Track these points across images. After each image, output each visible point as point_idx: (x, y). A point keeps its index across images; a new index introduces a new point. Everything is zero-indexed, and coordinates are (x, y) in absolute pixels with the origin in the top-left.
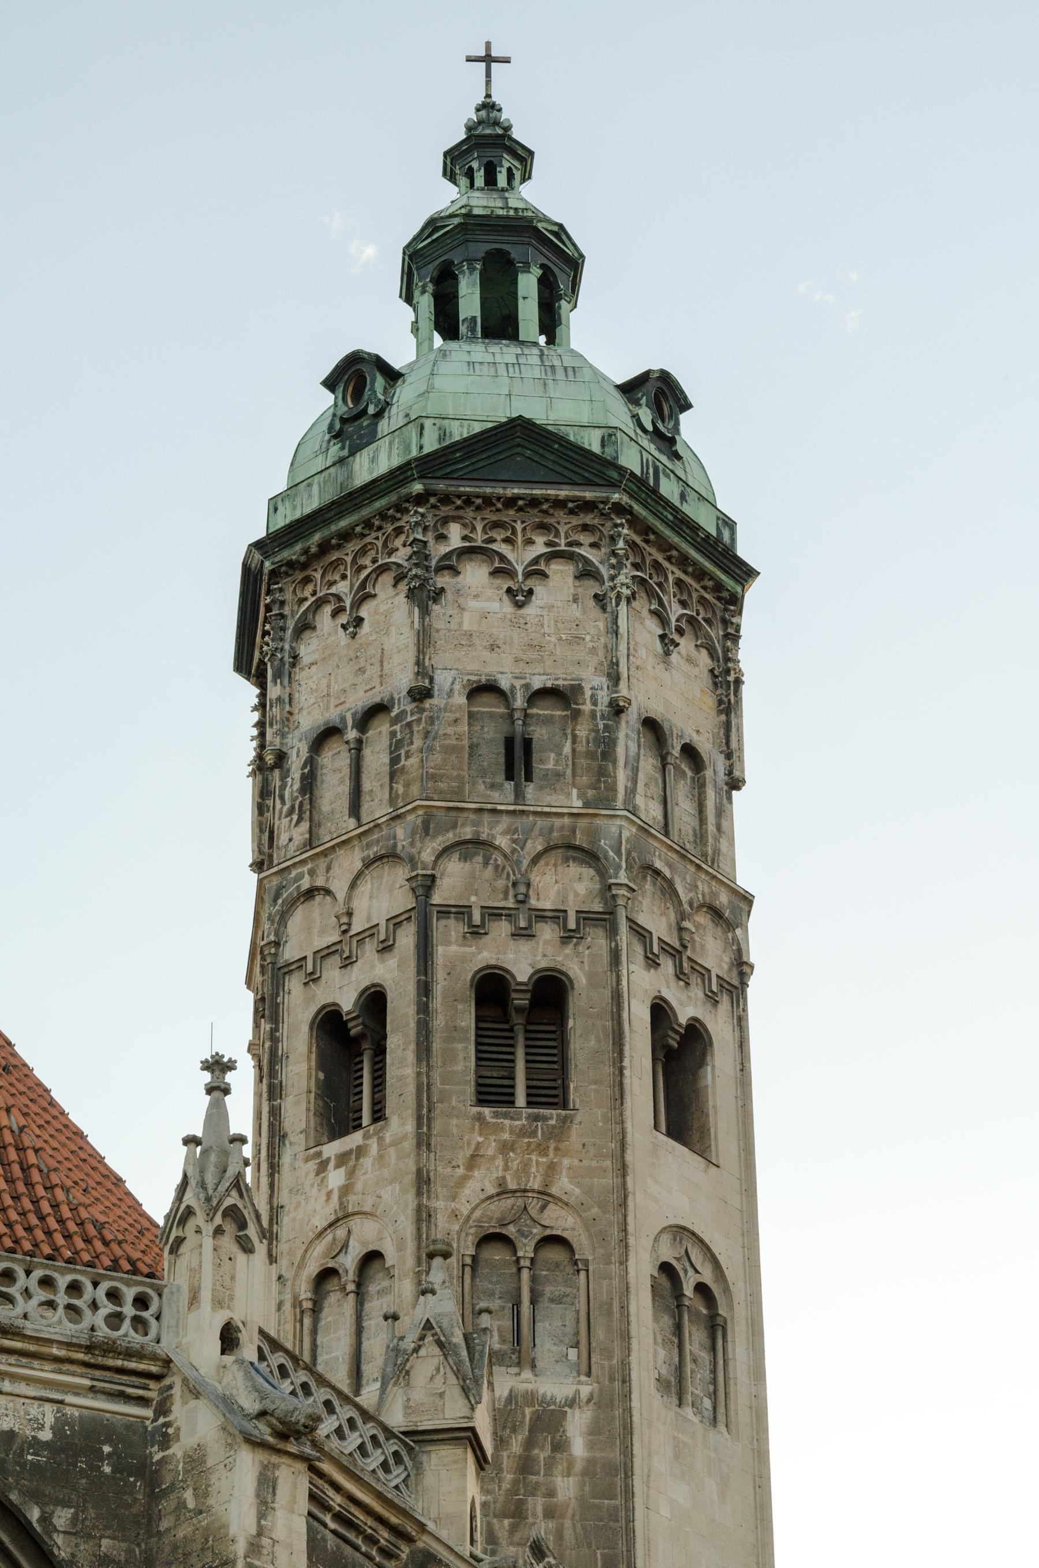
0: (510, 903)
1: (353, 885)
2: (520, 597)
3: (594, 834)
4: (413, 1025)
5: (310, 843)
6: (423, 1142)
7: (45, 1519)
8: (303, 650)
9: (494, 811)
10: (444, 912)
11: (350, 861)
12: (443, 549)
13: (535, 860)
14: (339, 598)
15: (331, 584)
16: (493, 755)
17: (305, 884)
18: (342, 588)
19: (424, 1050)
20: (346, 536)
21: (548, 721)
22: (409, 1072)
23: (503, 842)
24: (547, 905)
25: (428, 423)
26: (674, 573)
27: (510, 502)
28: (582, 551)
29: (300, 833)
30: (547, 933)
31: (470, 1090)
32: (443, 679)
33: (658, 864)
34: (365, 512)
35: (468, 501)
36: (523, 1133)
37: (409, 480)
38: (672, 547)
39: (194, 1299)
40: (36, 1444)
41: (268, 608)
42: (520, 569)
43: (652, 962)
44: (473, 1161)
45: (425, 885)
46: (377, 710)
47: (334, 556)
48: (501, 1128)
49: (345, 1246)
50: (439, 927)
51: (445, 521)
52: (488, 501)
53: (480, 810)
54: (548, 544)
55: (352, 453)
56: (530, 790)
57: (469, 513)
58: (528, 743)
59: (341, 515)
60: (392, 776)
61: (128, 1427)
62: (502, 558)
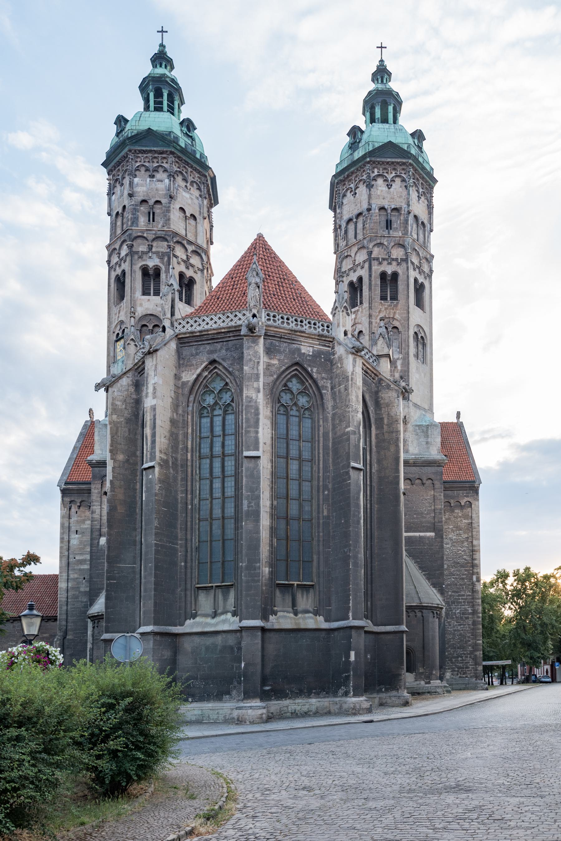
0: (387, 257)
1: (356, 254)
2: (389, 186)
3: (404, 241)
4: (368, 284)
5: (346, 245)
6: (370, 308)
8: (344, 201)
10: (374, 259)
11: (355, 249)
13: (392, 247)
14: (351, 188)
15: (350, 185)
16: (384, 224)
17: (346, 254)
19: (370, 289)
20: (353, 173)
21: (395, 216)
22: (367, 293)
23: (386, 243)
24: (394, 257)
25: (370, 143)
26: (421, 181)
27: (388, 163)
28: (403, 175)
29: (345, 243)
30: (394, 263)
31: (379, 297)
32: (373, 206)
33: (416, 248)
34: (357, 166)
35: (379, 162)
36: (389, 306)
37: (366, 158)
38: (421, 174)
41: (336, 191)
42: (389, 180)
43: (414, 270)
44: (380, 312)
45: (370, 253)
46: (360, 214)
48: (385, 305)
49: (355, 330)
50: (373, 262)
51: (374, 168)
52: (383, 163)
53: (381, 236)
54: (396, 173)
55: (354, 152)
56: (391, 232)
57: (379, 166)
58: (391, 221)
59: (352, 167)
60: (363, 229)
62: (386, 177)
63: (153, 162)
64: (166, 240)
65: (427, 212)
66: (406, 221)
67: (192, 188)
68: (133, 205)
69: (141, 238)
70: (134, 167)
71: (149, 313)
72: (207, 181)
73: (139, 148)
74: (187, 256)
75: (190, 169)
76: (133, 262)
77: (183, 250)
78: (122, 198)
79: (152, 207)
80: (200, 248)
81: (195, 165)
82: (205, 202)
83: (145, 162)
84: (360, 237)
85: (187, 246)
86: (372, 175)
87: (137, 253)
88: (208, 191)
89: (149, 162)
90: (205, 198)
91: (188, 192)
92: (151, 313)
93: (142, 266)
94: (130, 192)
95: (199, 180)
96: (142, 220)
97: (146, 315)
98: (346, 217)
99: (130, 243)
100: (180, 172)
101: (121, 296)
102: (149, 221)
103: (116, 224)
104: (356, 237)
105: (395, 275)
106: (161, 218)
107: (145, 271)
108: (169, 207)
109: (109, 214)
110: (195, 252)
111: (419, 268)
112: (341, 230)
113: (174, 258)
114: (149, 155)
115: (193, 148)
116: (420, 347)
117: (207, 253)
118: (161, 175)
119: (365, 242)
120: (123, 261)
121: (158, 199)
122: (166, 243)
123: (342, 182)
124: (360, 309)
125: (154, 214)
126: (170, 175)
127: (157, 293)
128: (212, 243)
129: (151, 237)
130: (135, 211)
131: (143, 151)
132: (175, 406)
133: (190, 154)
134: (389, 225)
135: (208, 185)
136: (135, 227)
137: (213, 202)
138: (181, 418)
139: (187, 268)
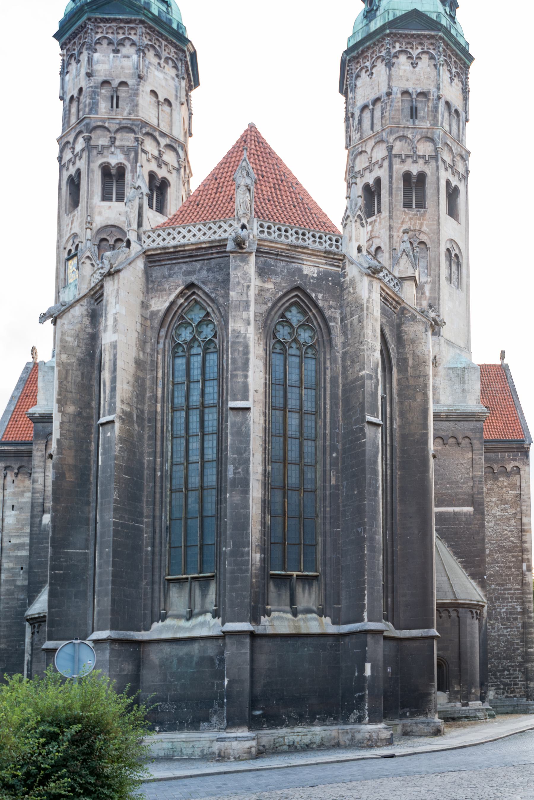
0: (412, 153)
1: (372, 150)
2: (414, 65)
3: (433, 133)
4: (388, 187)
5: (361, 138)
6: (391, 217)
7: (316, 297)
9: (408, 127)
10: (395, 156)
11: (371, 143)
12: (395, 51)
13: (418, 141)
14: (367, 67)
15: (365, 63)
16: (407, 112)
17: (360, 150)
18: (368, 64)
19: (390, 194)
20: (368, 48)
21: (421, 101)
22: (387, 199)
23: (410, 136)
24: (421, 153)
25: (390, 11)
27: (412, 36)
28: (431, 51)
29: (358, 136)
30: (421, 161)
31: (402, 204)
32: (395, 90)
33: (449, 143)
34: (374, 40)
35: (401, 35)
36: (415, 215)
39: (350, 239)
40: (313, 277)
41: (348, 71)
42: (415, 57)
43: (446, 169)
45: (390, 149)
46: (378, 100)
47: (365, 54)
51: (395, 42)
52: (406, 35)
53: (404, 127)
54: (422, 49)
55: (370, 22)
57: (401, 39)
59: (367, 41)
60: (382, 118)
61: (335, 273)
62: (410, 53)
63: (118, 33)
64: (133, 131)
65: (461, 97)
66: (436, 108)
67: (166, 66)
68: (92, 87)
69: (102, 129)
70: (94, 40)
71: (110, 223)
72: (186, 57)
73: (100, 16)
74: (160, 151)
75: (164, 43)
76: (91, 158)
77: (154, 144)
78: (78, 78)
79: (116, 90)
80: (176, 141)
81: (170, 38)
82: (184, 83)
83: (107, 33)
84: (378, 128)
85: (160, 139)
86: (393, 51)
87: (96, 147)
88: (187, 70)
89: (113, 33)
90: (183, 78)
91: (162, 71)
93: (102, 164)
94: (89, 71)
95: (175, 56)
96: (103, 106)
97: (107, 226)
98: (360, 103)
99: (87, 134)
100: (152, 46)
101: (75, 201)
102: (112, 107)
103: (70, 111)
104: (372, 128)
105: (422, 176)
106: (127, 104)
107: (106, 170)
108: (137, 89)
109: (62, 98)
110: (169, 146)
111: (452, 167)
112: (354, 120)
113: (143, 154)
114: (114, 24)
115: (169, 16)
116: (454, 267)
117: (184, 147)
118: (127, 50)
119: (384, 134)
120: (77, 158)
121: (124, 80)
122: (132, 135)
123: (355, 59)
124: (378, 219)
125: (118, 98)
126: (140, 49)
127: (120, 198)
128: (191, 135)
129: (113, 127)
130: (94, 94)
131: (106, 19)
132: (142, 343)
133: (165, 23)
134: (414, 113)
135: (187, 62)
136: (94, 114)
137: (192, 83)
138: (149, 358)
139: (159, 166)
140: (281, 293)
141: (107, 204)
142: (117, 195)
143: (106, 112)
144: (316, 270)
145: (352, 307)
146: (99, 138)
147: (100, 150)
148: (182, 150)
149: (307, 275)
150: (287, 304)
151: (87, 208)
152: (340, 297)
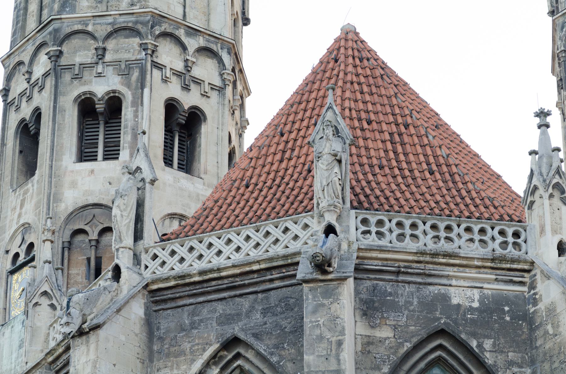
7: (480, 346)
39: (542, 231)
40: (471, 309)
61: (516, 297)
64: (138, 33)
69: (81, 35)
74: (186, 61)
76: (61, 88)
77: (176, 50)
87: (70, 67)
92: (96, 201)
93: (79, 96)
97: (85, 207)
103: (26, 9)
110: (205, 51)
120: (36, 89)
122: (137, 40)
128: (246, 22)
129: (101, 30)
139: (186, 88)
140: (408, 346)
141: (87, 166)
142: (105, 147)
143: (89, 7)
144: (476, 294)
145: (553, 363)
146: (75, 52)
147: (77, 72)
148: (229, 53)
149: (459, 305)
150: (422, 365)
151: (50, 177)
152: (531, 341)
